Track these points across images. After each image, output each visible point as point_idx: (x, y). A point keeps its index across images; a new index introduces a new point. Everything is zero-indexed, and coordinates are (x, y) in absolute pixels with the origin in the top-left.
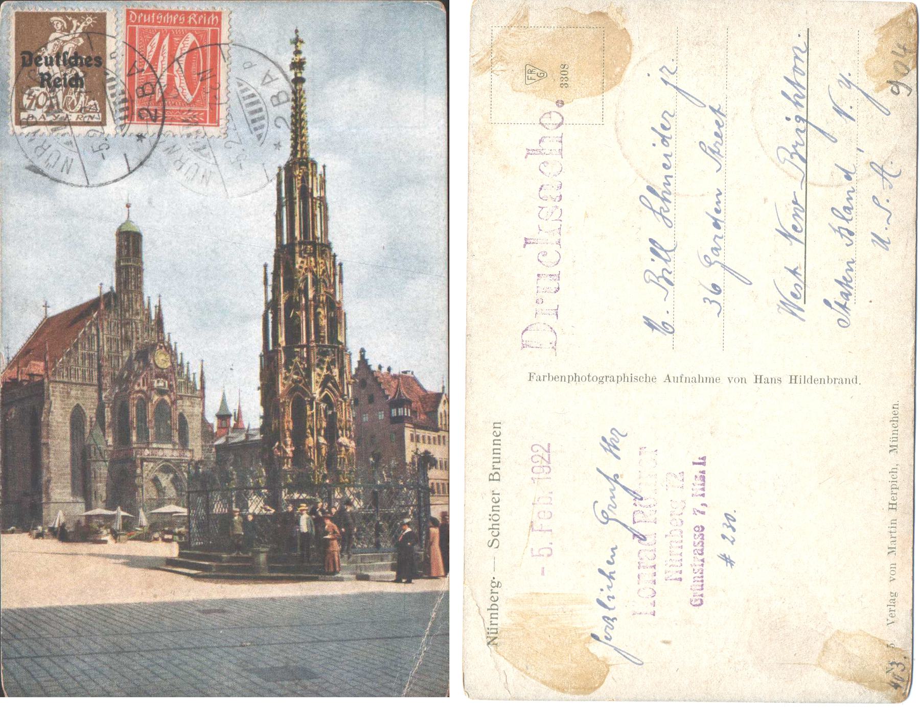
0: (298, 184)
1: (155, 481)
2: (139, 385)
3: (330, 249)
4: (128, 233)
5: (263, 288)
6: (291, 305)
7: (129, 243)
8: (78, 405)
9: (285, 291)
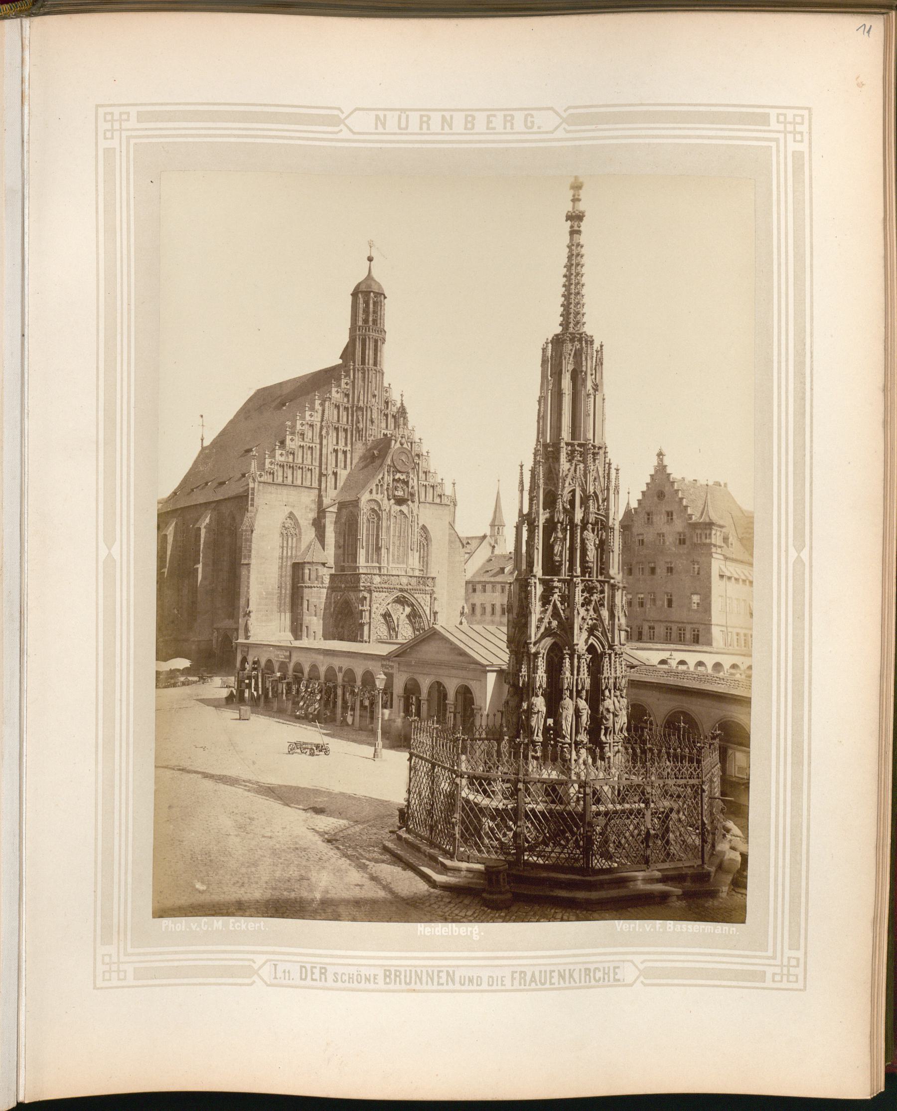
0: (568, 367)
1: (387, 616)
2: (371, 492)
3: (605, 453)
4: (367, 294)
5: (518, 493)
6: (550, 527)
7: (367, 301)
8: (291, 513)
9: (544, 509)
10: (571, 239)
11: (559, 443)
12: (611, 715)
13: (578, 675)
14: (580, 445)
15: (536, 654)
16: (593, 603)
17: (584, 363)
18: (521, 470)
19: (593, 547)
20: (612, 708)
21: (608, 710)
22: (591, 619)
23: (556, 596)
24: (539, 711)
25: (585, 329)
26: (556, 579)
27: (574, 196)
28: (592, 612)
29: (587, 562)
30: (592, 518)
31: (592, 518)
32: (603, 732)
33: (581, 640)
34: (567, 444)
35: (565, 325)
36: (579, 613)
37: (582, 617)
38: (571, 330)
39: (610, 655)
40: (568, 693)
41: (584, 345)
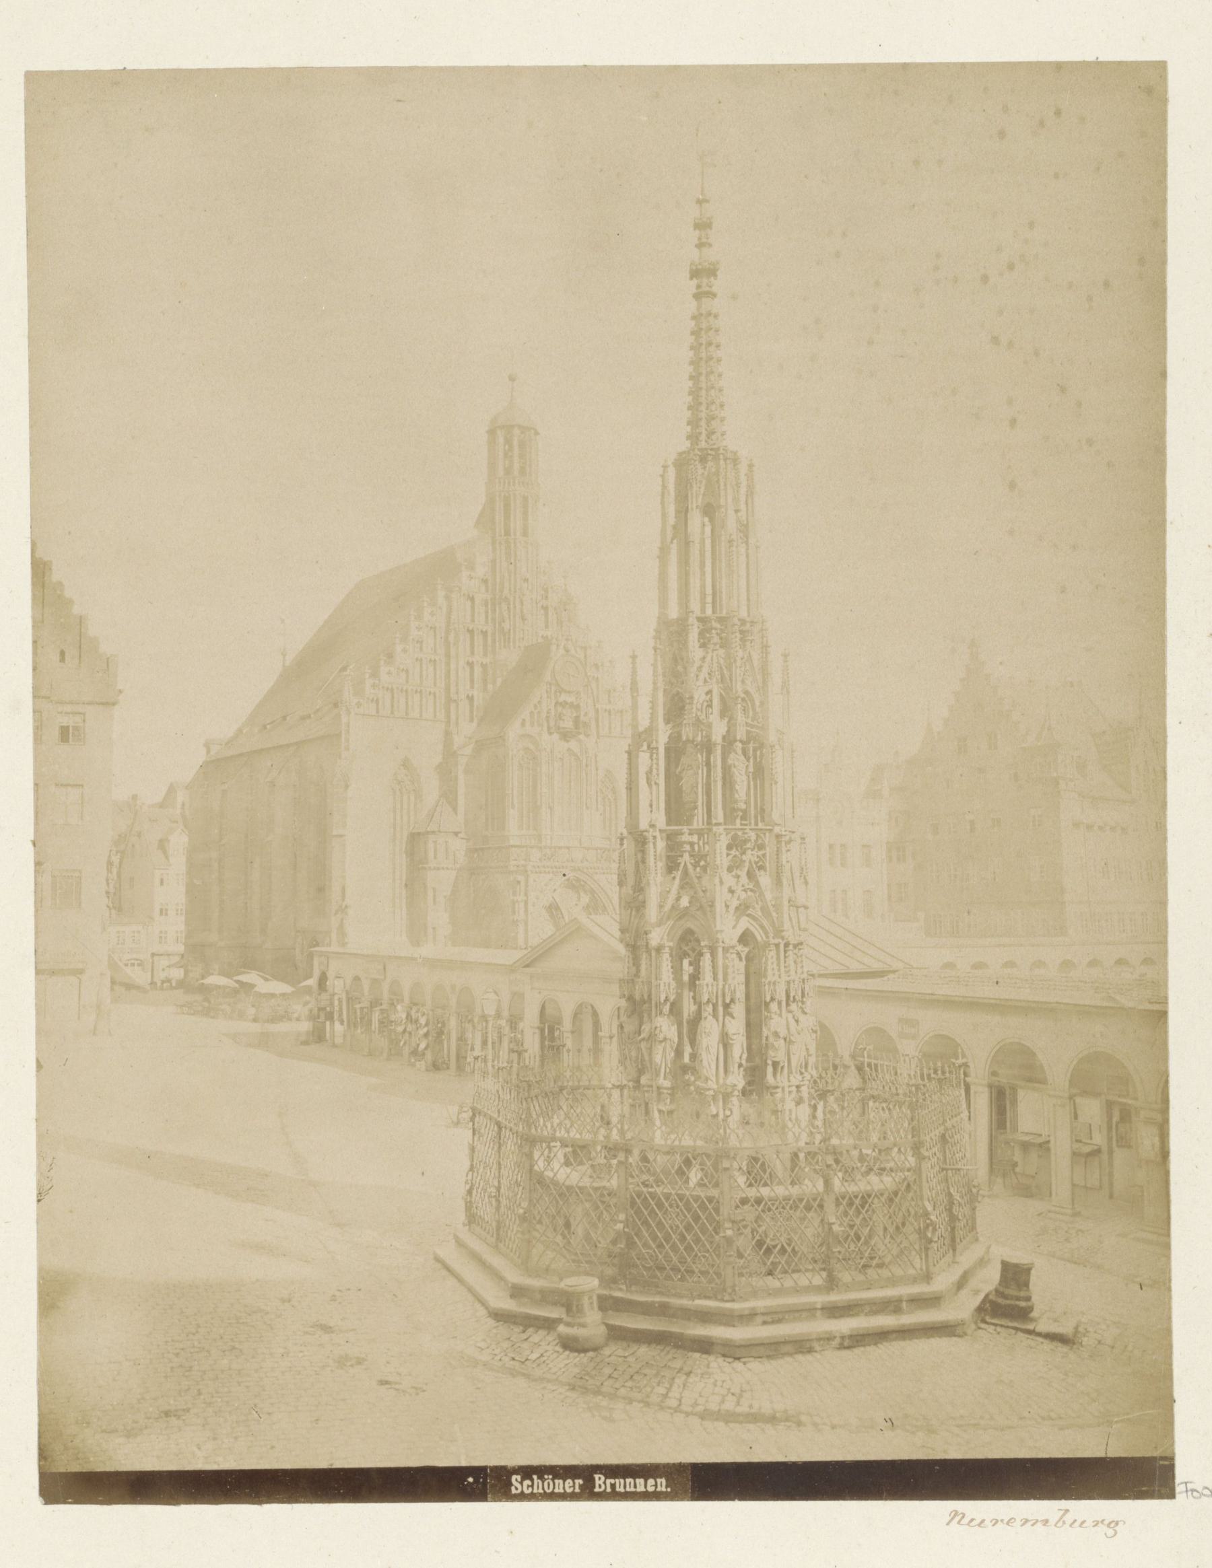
10: (699, 308)
11: (687, 620)
12: (782, 1041)
13: (726, 975)
14: (721, 620)
15: (659, 950)
16: (747, 864)
17: (722, 493)
18: (634, 663)
19: (744, 778)
20: (783, 1032)
21: (776, 1034)
22: (745, 891)
23: (686, 856)
24: (665, 1039)
25: (724, 443)
26: (685, 829)
27: (700, 239)
28: (744, 879)
29: (736, 802)
30: (741, 733)
31: (741, 733)
32: (770, 1069)
33: (728, 929)
34: (700, 619)
35: (693, 438)
36: (721, 883)
37: (724, 888)
38: (703, 444)
39: (777, 945)
40: (710, 1008)
41: (722, 462)
